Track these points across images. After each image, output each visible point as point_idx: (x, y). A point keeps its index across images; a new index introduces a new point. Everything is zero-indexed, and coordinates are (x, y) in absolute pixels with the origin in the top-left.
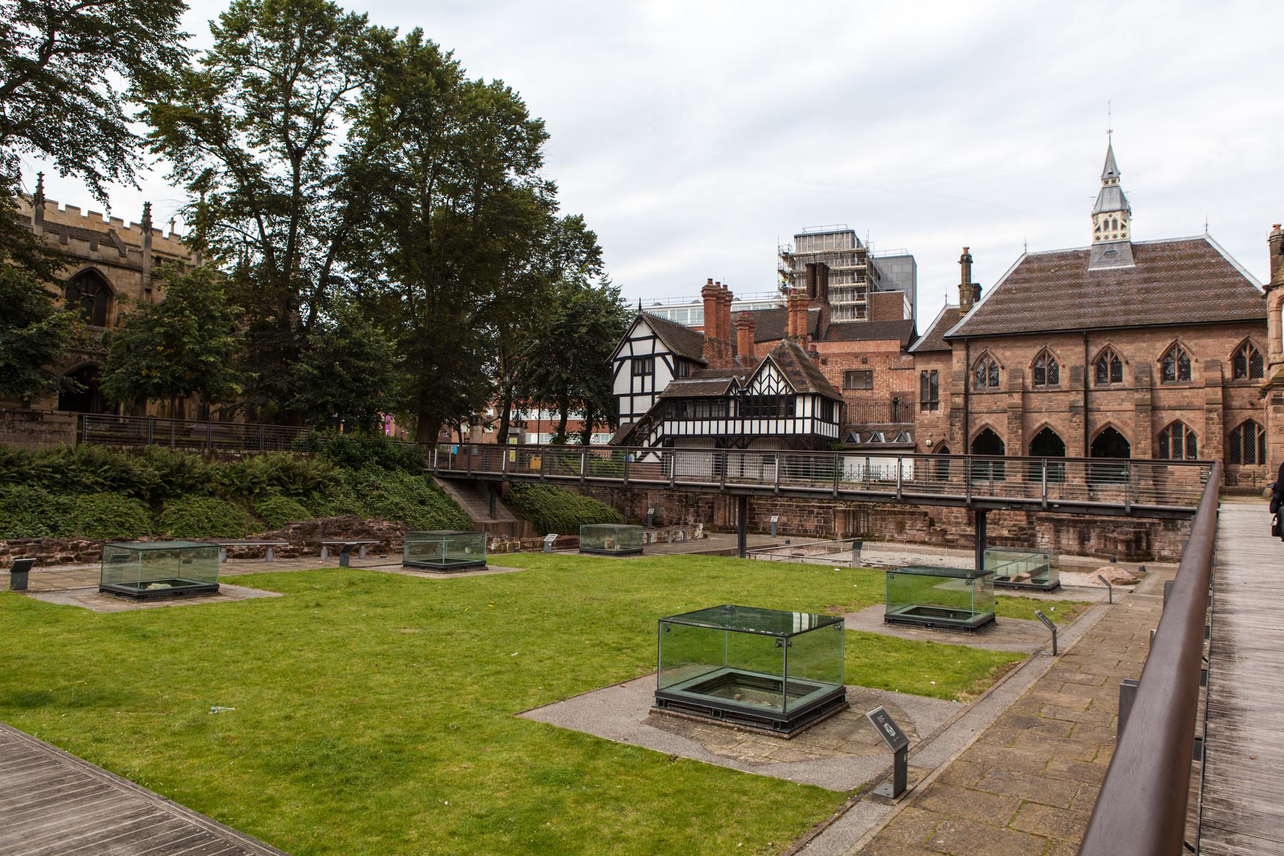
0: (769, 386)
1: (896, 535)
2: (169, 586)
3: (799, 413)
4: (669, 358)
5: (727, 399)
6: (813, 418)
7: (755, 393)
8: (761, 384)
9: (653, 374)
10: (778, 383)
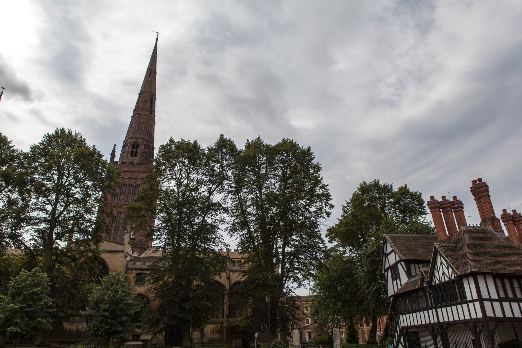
0: (444, 273)
3: (469, 298)
4: (403, 263)
5: (422, 289)
7: (437, 282)
8: (438, 272)
9: (399, 277)
10: (448, 269)
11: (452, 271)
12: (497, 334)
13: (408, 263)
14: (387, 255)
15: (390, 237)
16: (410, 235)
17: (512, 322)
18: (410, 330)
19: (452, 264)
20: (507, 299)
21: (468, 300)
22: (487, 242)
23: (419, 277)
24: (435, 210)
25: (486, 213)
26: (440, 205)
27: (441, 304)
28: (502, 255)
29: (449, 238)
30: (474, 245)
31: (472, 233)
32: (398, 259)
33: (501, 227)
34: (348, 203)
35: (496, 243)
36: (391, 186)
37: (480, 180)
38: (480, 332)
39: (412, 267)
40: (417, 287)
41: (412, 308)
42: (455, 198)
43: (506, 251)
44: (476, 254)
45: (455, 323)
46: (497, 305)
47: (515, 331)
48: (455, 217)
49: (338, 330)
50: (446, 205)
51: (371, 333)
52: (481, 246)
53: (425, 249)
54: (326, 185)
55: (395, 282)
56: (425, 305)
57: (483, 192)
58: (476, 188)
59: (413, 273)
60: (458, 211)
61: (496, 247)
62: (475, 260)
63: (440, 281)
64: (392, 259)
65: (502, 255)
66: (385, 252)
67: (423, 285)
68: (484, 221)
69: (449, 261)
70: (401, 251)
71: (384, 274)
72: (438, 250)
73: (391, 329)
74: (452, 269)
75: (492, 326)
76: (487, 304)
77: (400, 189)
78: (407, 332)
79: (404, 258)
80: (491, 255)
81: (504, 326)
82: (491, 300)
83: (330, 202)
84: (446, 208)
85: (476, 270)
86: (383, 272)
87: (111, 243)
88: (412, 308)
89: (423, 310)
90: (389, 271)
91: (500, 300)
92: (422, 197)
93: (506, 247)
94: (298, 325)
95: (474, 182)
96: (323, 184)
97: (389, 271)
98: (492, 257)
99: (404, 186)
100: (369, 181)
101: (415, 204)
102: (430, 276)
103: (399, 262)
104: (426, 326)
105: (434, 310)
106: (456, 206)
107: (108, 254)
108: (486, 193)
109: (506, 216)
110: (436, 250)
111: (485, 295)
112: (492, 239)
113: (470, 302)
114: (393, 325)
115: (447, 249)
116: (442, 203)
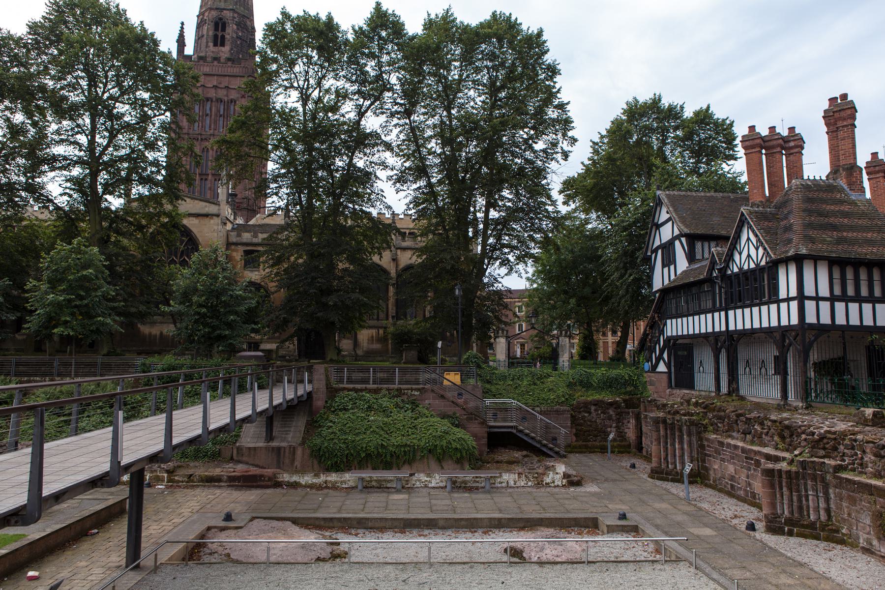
0: (749, 256)
1: (875, 542)
2: (286, 477)
3: (782, 294)
4: (683, 239)
5: (709, 280)
6: (801, 298)
7: (736, 270)
8: (740, 254)
10: (757, 249)
11: (764, 253)
12: (815, 348)
13: (692, 239)
14: (658, 226)
15: (668, 196)
16: (703, 194)
17: (843, 332)
18: (680, 341)
19: (766, 241)
20: (845, 299)
21: (780, 298)
22: (832, 207)
23: (706, 263)
24: (754, 150)
25: (841, 157)
26: (764, 141)
27: (736, 304)
28: (852, 228)
29: (769, 200)
30: (809, 212)
31: (810, 191)
32: (676, 232)
33: (862, 182)
34: (602, 137)
35: (846, 208)
36: (682, 107)
37: (844, 96)
38: (790, 345)
39: (698, 245)
40: (702, 277)
41: (688, 308)
42: (792, 129)
43: (860, 222)
44: (810, 226)
45: (753, 331)
46: (825, 306)
47: (844, 344)
48: (785, 164)
49: (567, 339)
50: (775, 142)
51: (618, 346)
52: (821, 214)
53: (725, 217)
54: (565, 102)
55: (666, 270)
56: (709, 305)
57: (844, 119)
58: (834, 112)
59: (699, 256)
60: (792, 154)
61: (846, 215)
62: (805, 236)
63: (741, 269)
64: (666, 233)
65: (852, 228)
66: (656, 221)
67: (711, 274)
68: (835, 171)
69: (762, 236)
70: (683, 221)
71: (651, 256)
72: (746, 219)
73: (650, 340)
74: (765, 249)
75: (810, 336)
76: (810, 306)
77: (697, 114)
78: (674, 344)
79: (686, 231)
80: (834, 228)
81: (829, 337)
82: (817, 299)
83: (570, 134)
84: (773, 147)
85: (804, 251)
86: (649, 254)
87: (196, 202)
88: (688, 308)
89: (705, 312)
90: (660, 252)
91: (832, 299)
92: (733, 128)
93: (863, 215)
94: (505, 332)
95: (832, 100)
96: (560, 100)
97: (660, 252)
98: (835, 231)
99: (705, 107)
100: (644, 97)
101: (720, 141)
102: (725, 260)
103: (678, 237)
104: (706, 336)
105: (723, 313)
106: (792, 144)
107: (194, 219)
108: (849, 122)
109: (874, 164)
110: (743, 218)
111: (809, 290)
112: (841, 202)
113: (783, 300)
114: (655, 333)
115: (761, 217)
116: (767, 139)
